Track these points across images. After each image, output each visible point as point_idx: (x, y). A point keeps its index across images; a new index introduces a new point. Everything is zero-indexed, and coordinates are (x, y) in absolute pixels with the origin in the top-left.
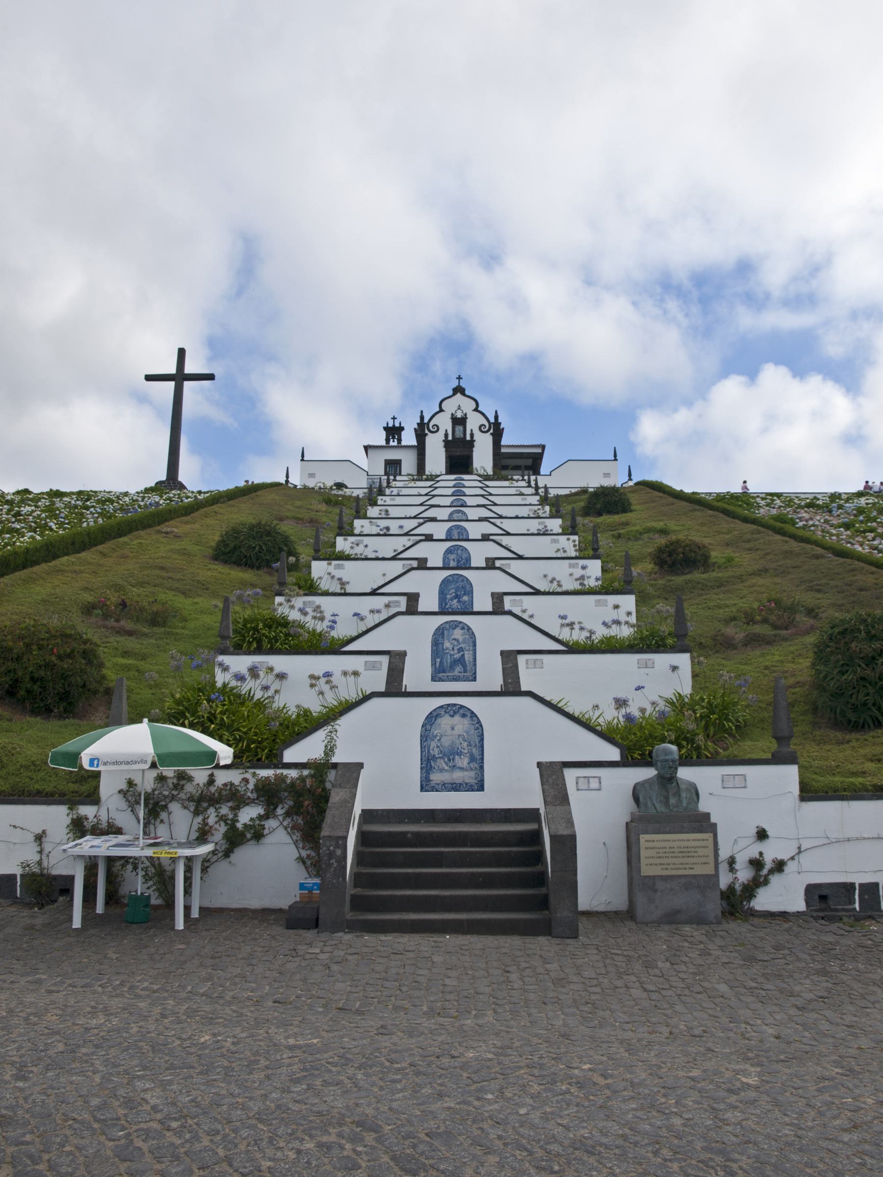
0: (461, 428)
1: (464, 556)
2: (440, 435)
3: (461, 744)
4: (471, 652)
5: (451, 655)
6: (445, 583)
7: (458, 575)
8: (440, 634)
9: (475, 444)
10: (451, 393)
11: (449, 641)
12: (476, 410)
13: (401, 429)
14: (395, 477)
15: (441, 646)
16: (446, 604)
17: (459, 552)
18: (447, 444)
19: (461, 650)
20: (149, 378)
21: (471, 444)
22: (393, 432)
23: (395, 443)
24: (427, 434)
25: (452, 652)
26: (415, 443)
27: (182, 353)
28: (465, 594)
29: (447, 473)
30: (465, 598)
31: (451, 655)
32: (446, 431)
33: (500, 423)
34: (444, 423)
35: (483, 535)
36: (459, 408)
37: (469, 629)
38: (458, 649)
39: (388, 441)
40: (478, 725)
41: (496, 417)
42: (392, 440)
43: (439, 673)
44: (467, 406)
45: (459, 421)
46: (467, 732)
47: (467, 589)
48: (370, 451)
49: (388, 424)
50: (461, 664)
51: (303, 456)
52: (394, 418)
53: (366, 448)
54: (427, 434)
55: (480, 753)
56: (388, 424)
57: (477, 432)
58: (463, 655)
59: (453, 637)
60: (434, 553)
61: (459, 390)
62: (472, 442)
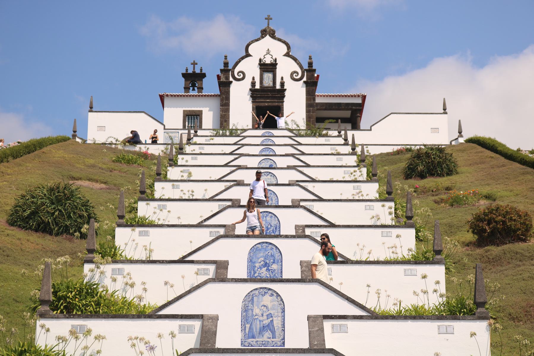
0: (270, 75)
1: (274, 222)
2: (246, 85)
4: (280, 318)
5: (260, 321)
6: (254, 249)
7: (267, 243)
8: (250, 298)
9: (286, 93)
11: (258, 308)
12: (287, 55)
13: (202, 76)
14: (196, 132)
15: (250, 312)
16: (255, 273)
17: (268, 218)
19: (270, 316)
24: (231, 82)
25: (261, 318)
26: (218, 93)
28: (274, 262)
29: (254, 128)
30: (274, 267)
31: (260, 321)
32: (253, 78)
35: (293, 201)
36: (268, 52)
37: (278, 295)
38: (267, 315)
39: (187, 89)
41: (310, 64)
42: (191, 88)
43: (249, 338)
49: (187, 70)
50: (270, 330)
51: (91, 108)
52: (194, 64)
54: (231, 82)
56: (187, 70)
58: (272, 321)
59: (262, 304)
62: (282, 91)
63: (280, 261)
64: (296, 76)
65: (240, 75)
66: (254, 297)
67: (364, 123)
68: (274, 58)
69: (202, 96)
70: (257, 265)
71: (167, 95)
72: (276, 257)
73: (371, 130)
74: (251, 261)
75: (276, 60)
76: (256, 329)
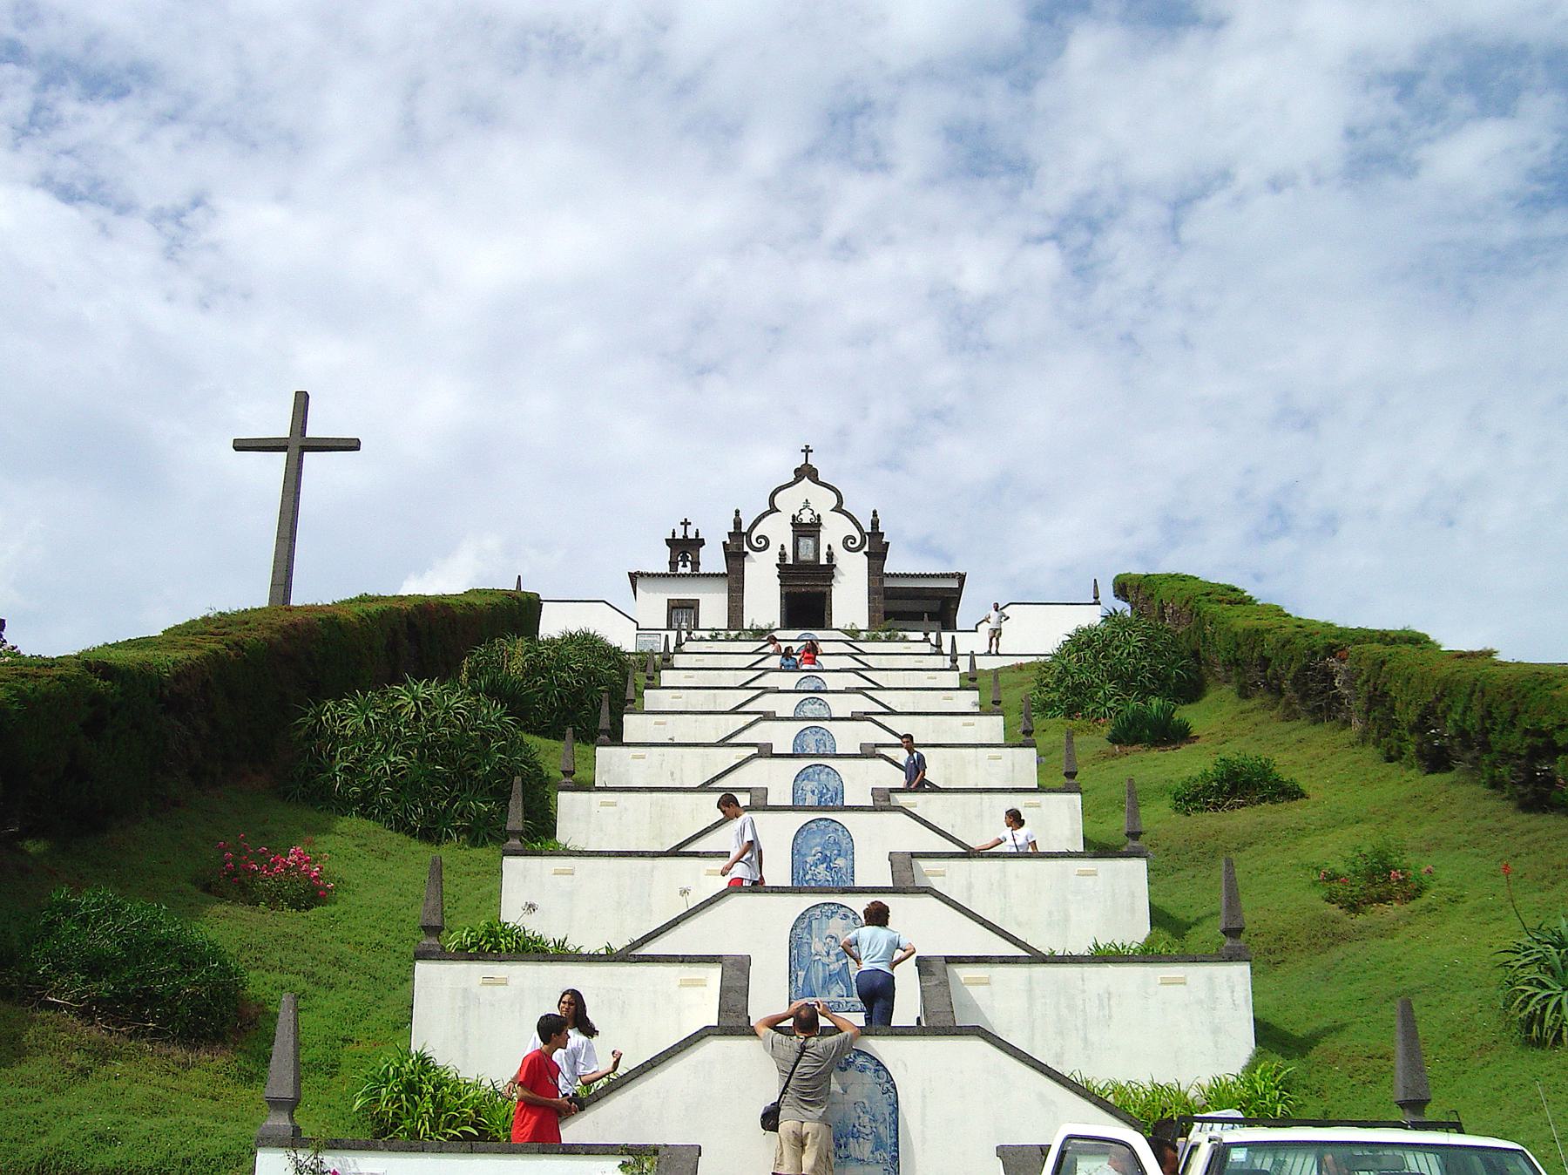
0: (810, 542)
1: (832, 784)
2: (772, 556)
3: (859, 1117)
7: (826, 819)
10: (792, 477)
11: (820, 940)
12: (838, 509)
13: (701, 543)
14: (689, 634)
15: (806, 947)
17: (823, 777)
18: (789, 572)
20: (241, 446)
21: (826, 573)
22: (684, 548)
23: (688, 570)
24: (747, 553)
25: (826, 960)
27: (302, 400)
28: (839, 855)
30: (840, 862)
32: (782, 546)
33: (883, 533)
34: (778, 531)
35: (862, 746)
38: (837, 955)
39: (673, 564)
40: (888, 1085)
41: (875, 524)
42: (681, 564)
44: (822, 502)
45: (806, 530)
46: (869, 1098)
47: (843, 846)
48: (639, 582)
49: (674, 533)
50: (842, 981)
52: (686, 523)
53: (634, 577)
55: (893, 1133)
56: (674, 533)
57: (839, 551)
59: (827, 934)
60: (777, 779)
61: (806, 472)
63: (849, 852)
64: (851, 543)
65: (761, 542)
66: (813, 922)
67: (963, 617)
68: (816, 515)
69: (698, 575)
70: (810, 859)
71: (642, 575)
72: (844, 846)
73: (976, 631)
74: (796, 851)
75: (819, 516)
76: (817, 979)
